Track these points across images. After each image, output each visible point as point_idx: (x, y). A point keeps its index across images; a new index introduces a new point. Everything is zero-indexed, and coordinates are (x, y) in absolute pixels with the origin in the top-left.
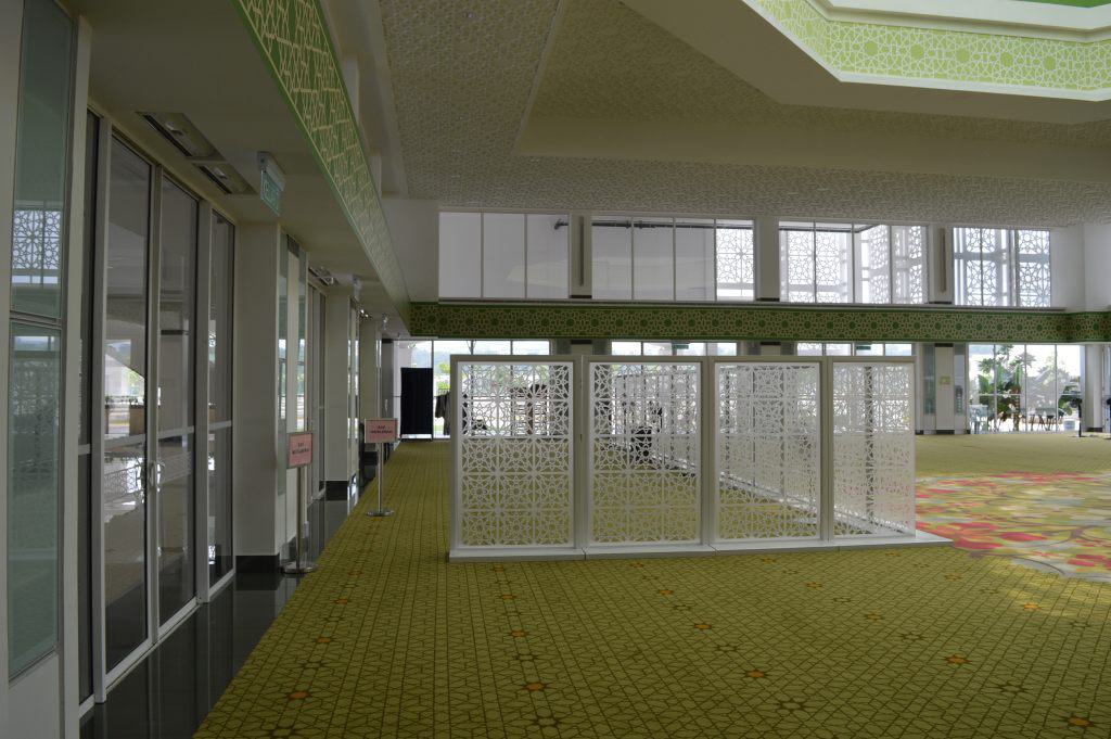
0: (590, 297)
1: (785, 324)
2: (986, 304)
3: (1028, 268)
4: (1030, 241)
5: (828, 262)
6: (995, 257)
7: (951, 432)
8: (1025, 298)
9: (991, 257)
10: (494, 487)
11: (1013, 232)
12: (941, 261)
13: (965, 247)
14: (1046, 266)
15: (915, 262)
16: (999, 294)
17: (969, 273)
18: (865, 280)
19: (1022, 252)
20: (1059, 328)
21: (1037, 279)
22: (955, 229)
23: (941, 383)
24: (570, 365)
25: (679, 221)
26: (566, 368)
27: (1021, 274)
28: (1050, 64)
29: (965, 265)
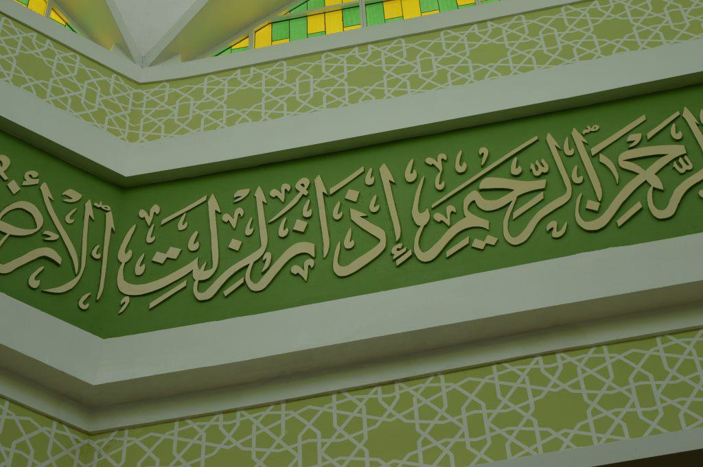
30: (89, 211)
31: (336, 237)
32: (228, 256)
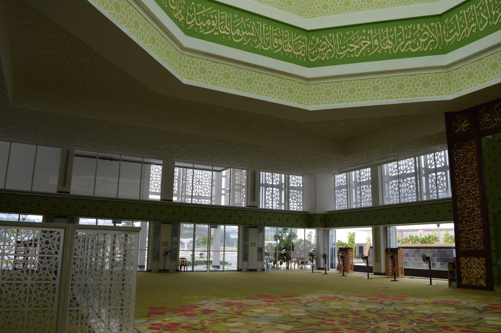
0: (69, 193)
2: (274, 208)
3: (294, 193)
4: (295, 181)
5: (200, 184)
6: (279, 186)
7: (255, 270)
8: (292, 207)
9: (277, 186)
10: (25, 292)
11: (287, 176)
12: (254, 187)
13: (266, 181)
14: (301, 192)
15: (243, 187)
16: (280, 204)
17: (267, 193)
19: (292, 185)
20: (305, 221)
21: (297, 198)
22: (261, 172)
23: (251, 246)
24: (62, 231)
25: (123, 157)
26: (58, 233)
27: (290, 195)
28: (291, 91)
29: (265, 190)
30: (436, 25)
31: (479, 21)
32: (462, 29)
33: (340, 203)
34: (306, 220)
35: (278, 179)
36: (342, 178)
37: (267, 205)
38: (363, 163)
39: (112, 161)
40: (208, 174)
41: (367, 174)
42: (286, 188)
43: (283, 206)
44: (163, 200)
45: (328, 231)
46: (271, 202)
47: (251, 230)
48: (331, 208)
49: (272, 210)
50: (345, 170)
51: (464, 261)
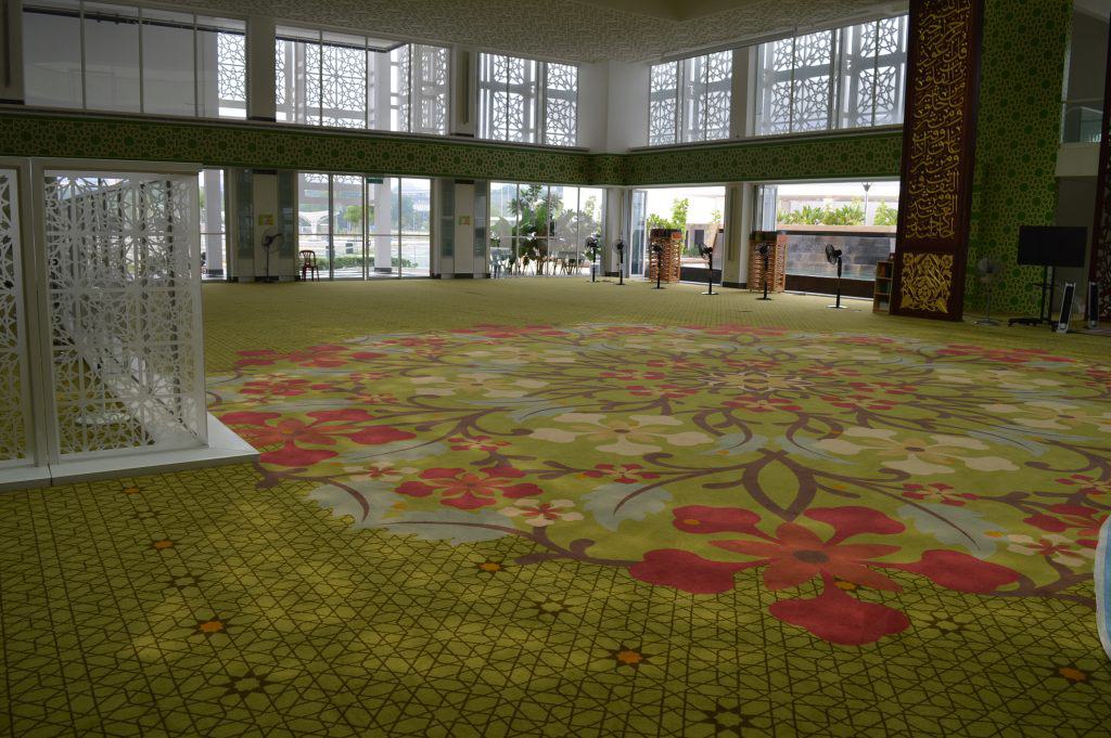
0: (22, 102)
1: (281, 150)
2: (512, 139)
3: (556, 105)
4: (560, 77)
6: (523, 90)
7: (470, 276)
8: (552, 137)
9: (517, 89)
11: (541, 63)
12: (465, 90)
13: (492, 76)
14: (574, 104)
15: (440, 89)
16: (526, 130)
18: (394, 107)
19: (551, 87)
20: (581, 170)
25: (148, 13)
27: (548, 110)
29: (492, 96)
33: (660, 131)
34: (584, 167)
35: (522, 71)
36: (666, 73)
37: (495, 132)
38: (718, 39)
39: (121, 24)
40: (355, 58)
41: (725, 65)
42: (538, 93)
43: (532, 135)
44: (254, 118)
45: (630, 192)
46: (504, 126)
47: (457, 186)
48: (637, 142)
49: (506, 143)
50: (676, 53)
51: (910, 259)
